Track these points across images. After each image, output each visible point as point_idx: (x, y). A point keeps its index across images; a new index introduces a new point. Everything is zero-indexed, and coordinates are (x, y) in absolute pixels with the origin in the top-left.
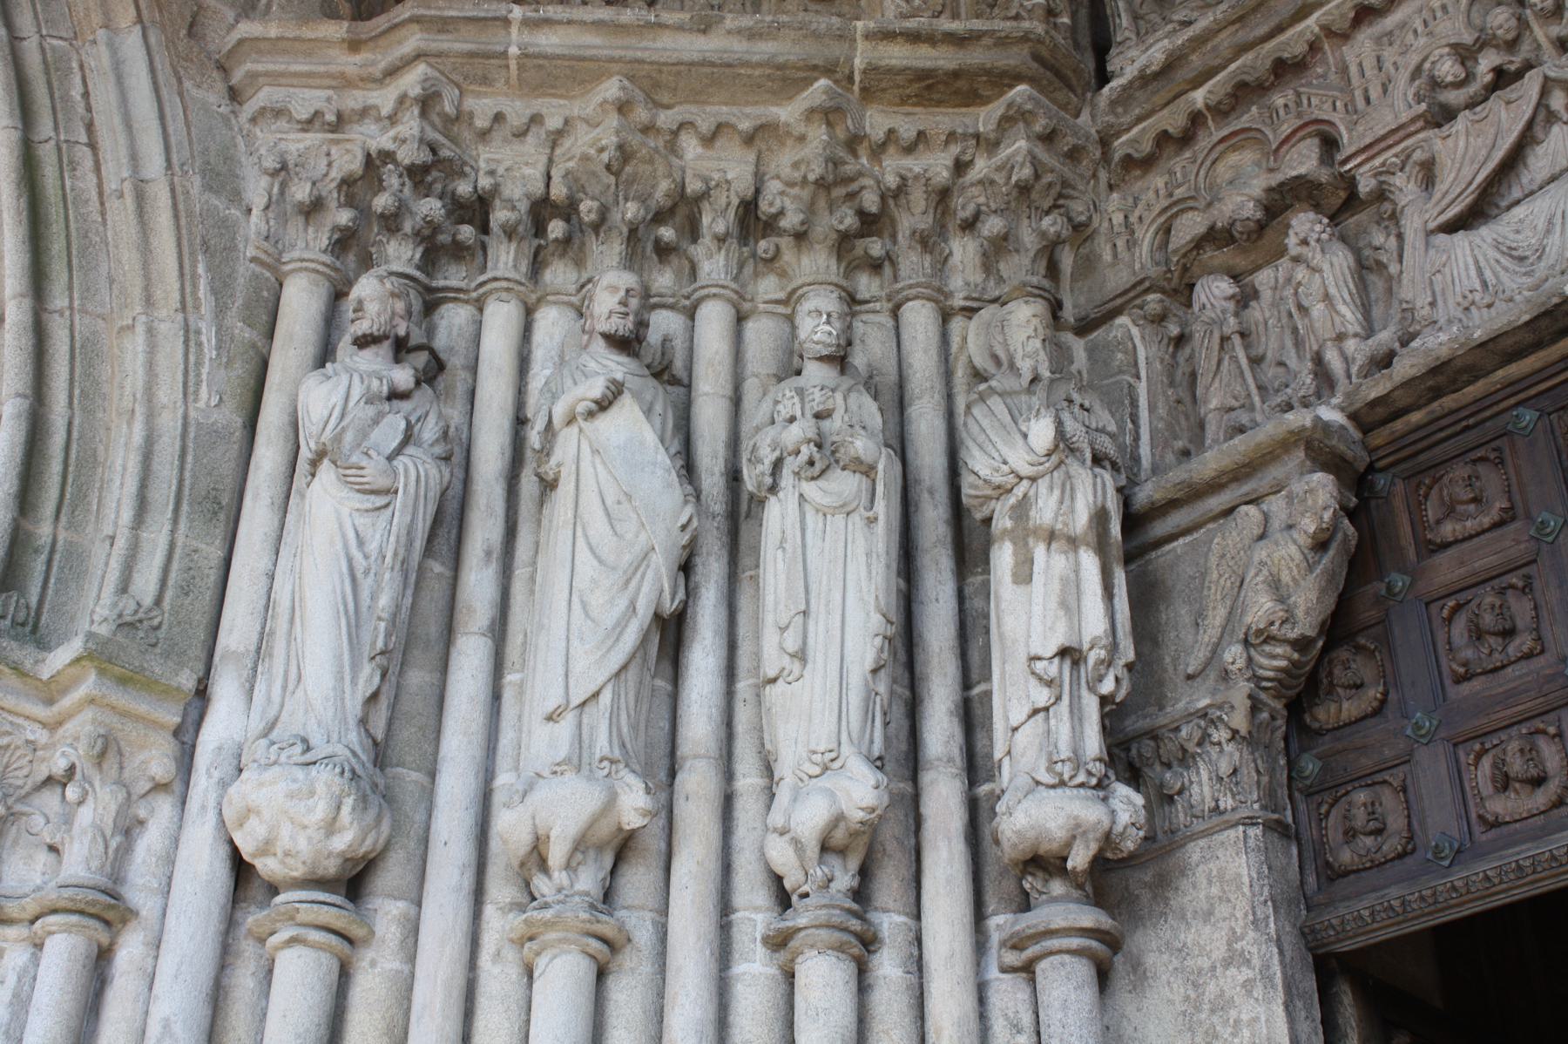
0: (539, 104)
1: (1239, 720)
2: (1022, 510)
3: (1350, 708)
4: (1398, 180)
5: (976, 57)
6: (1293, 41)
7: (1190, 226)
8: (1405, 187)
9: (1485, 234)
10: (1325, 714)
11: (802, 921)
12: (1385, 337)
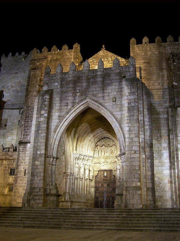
7: (96, 162)
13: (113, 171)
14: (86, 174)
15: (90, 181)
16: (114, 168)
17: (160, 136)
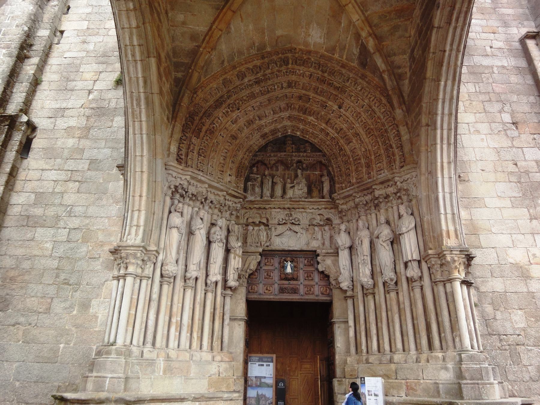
0: (198, 184)
1: (247, 277)
2: (235, 251)
5: (240, 195)
6: (267, 206)
7: (250, 220)
8: (273, 229)
10: (251, 276)
11: (210, 289)
12: (268, 244)
13: (318, 255)
15: (229, 292)
16: (323, 244)
17: (513, 123)
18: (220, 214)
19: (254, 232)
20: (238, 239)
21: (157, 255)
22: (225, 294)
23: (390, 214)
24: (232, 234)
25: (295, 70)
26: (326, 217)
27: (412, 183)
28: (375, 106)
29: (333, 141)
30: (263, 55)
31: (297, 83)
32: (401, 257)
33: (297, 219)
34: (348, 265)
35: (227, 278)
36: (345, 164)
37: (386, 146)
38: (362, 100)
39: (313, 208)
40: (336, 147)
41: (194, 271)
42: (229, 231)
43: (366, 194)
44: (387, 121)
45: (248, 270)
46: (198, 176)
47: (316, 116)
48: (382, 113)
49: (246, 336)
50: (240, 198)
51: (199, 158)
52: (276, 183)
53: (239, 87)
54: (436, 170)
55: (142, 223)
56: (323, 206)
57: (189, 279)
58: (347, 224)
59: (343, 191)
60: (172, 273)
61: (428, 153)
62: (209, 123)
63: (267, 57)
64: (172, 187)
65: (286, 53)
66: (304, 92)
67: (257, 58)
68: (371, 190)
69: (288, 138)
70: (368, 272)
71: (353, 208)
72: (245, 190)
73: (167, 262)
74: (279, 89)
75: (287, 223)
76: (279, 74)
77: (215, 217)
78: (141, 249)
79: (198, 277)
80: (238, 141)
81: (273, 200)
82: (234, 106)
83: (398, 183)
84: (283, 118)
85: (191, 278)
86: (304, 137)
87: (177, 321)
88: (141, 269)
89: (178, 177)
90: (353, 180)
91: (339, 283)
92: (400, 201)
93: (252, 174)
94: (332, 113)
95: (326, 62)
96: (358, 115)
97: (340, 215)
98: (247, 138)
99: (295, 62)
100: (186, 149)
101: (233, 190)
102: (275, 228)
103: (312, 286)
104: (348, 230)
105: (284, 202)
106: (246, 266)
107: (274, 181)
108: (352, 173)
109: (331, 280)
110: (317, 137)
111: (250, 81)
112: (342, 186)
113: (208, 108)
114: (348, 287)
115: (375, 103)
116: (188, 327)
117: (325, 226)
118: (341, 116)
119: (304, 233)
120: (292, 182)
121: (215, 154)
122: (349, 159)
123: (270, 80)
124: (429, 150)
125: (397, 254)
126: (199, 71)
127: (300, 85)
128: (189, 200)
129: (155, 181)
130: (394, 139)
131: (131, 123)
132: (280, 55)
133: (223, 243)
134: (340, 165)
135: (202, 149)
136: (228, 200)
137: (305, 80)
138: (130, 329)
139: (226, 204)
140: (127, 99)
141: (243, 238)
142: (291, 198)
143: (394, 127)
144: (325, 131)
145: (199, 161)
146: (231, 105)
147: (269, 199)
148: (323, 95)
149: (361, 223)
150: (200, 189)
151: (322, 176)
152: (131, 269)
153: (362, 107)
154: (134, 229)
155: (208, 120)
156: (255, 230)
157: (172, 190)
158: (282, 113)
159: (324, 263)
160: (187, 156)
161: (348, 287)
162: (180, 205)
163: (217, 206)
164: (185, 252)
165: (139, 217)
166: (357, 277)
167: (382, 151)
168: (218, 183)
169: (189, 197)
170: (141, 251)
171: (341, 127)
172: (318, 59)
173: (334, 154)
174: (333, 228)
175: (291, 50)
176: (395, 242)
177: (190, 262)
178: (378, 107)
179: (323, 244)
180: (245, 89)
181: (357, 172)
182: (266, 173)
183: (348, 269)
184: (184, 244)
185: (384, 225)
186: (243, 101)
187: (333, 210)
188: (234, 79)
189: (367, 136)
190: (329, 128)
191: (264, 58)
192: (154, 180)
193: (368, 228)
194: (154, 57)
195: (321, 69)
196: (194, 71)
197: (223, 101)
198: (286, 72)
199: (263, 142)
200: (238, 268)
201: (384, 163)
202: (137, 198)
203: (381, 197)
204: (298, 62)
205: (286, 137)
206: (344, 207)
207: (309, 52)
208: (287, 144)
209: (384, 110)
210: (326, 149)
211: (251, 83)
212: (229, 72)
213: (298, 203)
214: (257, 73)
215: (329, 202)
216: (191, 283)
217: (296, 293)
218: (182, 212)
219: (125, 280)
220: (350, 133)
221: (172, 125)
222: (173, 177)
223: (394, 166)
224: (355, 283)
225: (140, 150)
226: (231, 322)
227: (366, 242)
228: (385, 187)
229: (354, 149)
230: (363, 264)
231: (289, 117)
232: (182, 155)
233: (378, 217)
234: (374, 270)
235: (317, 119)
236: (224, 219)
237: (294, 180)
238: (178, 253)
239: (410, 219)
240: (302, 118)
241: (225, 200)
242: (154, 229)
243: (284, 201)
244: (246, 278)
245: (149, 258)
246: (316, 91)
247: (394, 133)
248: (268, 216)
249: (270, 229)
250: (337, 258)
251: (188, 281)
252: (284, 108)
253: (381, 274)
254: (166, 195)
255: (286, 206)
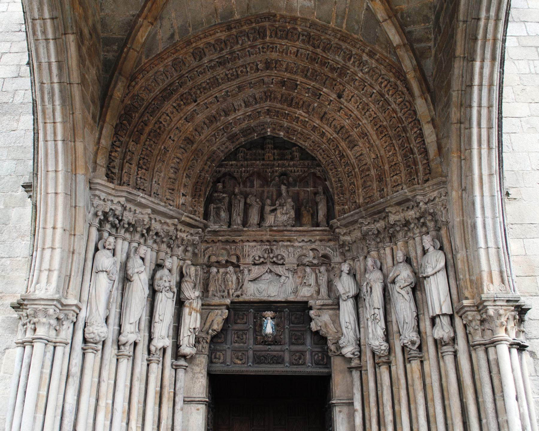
0: (136, 208)
1: (208, 341)
2: (191, 303)
3: (219, 341)
4: (246, 269)
7: (213, 259)
8: (246, 272)
9: (256, 286)
10: (215, 340)
12: (239, 293)
13: (311, 308)
14: (157, 318)
15: (182, 362)
16: (318, 292)
18: (169, 250)
19: (220, 276)
20: (195, 287)
21: (78, 311)
22: (176, 366)
23: (412, 249)
24: (187, 279)
25: (275, 45)
26: (322, 252)
27: (440, 204)
28: (388, 95)
29: (331, 144)
30: (229, 26)
31: (279, 63)
32: (426, 310)
33: (280, 257)
34: (352, 322)
35: (180, 343)
36: (348, 177)
37: (404, 151)
38: (371, 86)
39: (303, 241)
40: (335, 152)
41: (132, 333)
42: (182, 275)
43: (378, 219)
44: (406, 115)
45: (210, 331)
46: (136, 197)
47: (306, 109)
48: (399, 105)
49: (208, 425)
50: (198, 227)
51: (139, 172)
52: (250, 205)
53: (196, 69)
54: (472, 185)
55: (56, 265)
56: (318, 237)
57: (124, 345)
58: (351, 263)
59: (346, 215)
60: (100, 336)
61: (461, 162)
62: (153, 122)
63: (235, 28)
64: (100, 213)
65: (262, 22)
66: (288, 75)
67: (221, 29)
68: (384, 215)
69: (268, 141)
70: (380, 332)
71: (360, 239)
72: (206, 216)
73: (92, 320)
74: (253, 71)
75: (266, 263)
76: (252, 50)
77: (162, 255)
78: (55, 303)
79: (137, 341)
80: (195, 146)
81: (245, 229)
82: (190, 97)
83: (421, 204)
84: (259, 113)
85: (127, 342)
86: (290, 138)
87: (107, 404)
88: (55, 331)
89: (108, 200)
90: (359, 200)
91: (339, 348)
92: (424, 229)
93: (216, 192)
94: (329, 104)
95: (318, 33)
96: (365, 108)
97: (341, 250)
98: (208, 141)
99: (275, 33)
100: (120, 159)
101: (188, 217)
102: (249, 271)
103: (302, 353)
104: (352, 271)
105: (262, 233)
106: (208, 324)
107: (248, 201)
108: (358, 190)
109: (330, 344)
110: (309, 138)
111: (211, 61)
112: (343, 209)
113: (152, 101)
114: (353, 354)
115: (389, 90)
116: (123, 413)
117: (321, 265)
118: (341, 108)
119: (290, 276)
120: (273, 204)
121: (162, 165)
122: (354, 169)
123: (239, 59)
124: (463, 157)
125: (421, 306)
126: (138, 50)
127: (283, 65)
128: (125, 232)
129: (75, 207)
130: (415, 141)
131: (41, 125)
132: (254, 25)
133: (174, 293)
134: (341, 179)
135: (144, 158)
136: (181, 231)
137: (290, 59)
138: (40, 416)
139: (178, 237)
140: (35, 92)
141: (204, 285)
142: (272, 226)
143: (415, 124)
144: (320, 130)
145: (139, 176)
146: (185, 96)
147: (241, 227)
148: (316, 79)
149: (370, 262)
150: (140, 216)
151: (315, 194)
152: (41, 332)
153: (371, 96)
154: (45, 274)
155: (152, 118)
156: (221, 273)
157: (99, 217)
158: (258, 105)
159: (319, 318)
160: (122, 170)
161: (353, 354)
162: (111, 239)
163: (165, 240)
164: (118, 306)
165: (52, 257)
166: (365, 339)
167: (400, 158)
168: (165, 207)
169: (124, 227)
170: (55, 305)
171: (342, 125)
172: (307, 29)
173: (332, 162)
174: (333, 268)
175: (268, 18)
176: (418, 288)
177: (125, 320)
178: (392, 95)
179: (318, 292)
180: (204, 72)
181: (365, 188)
182: (237, 190)
183: (353, 327)
184: (116, 294)
185: (402, 264)
186: (202, 90)
187: (331, 244)
188: (189, 59)
189: (378, 136)
190: (325, 126)
191: (231, 28)
192: (74, 205)
193: (381, 269)
194: (73, 33)
195: (311, 43)
196: (131, 50)
197: (174, 90)
198: (263, 48)
199: (232, 147)
200: (194, 329)
201: (403, 175)
202: (49, 231)
203: (398, 223)
204: (279, 34)
205: (264, 138)
206: (348, 238)
207: (294, 19)
208: (266, 148)
209: (401, 99)
210: (321, 155)
211: (213, 65)
212: (182, 49)
213: (281, 234)
214: (222, 50)
215: (325, 231)
216: (127, 350)
217: (280, 363)
218: (114, 250)
219: (33, 346)
220: (354, 133)
221: (100, 125)
222: (100, 199)
223: (416, 180)
224: (362, 347)
225: (54, 163)
226: (186, 406)
227: (378, 289)
228: (403, 210)
229: (361, 155)
230: (373, 320)
231: (268, 110)
232: (114, 167)
233: (394, 254)
234: (390, 328)
235: (307, 112)
236: (175, 258)
237: (276, 201)
238: (108, 308)
239: (438, 256)
240: (287, 112)
241: (177, 230)
242: (73, 274)
243: (262, 231)
244: (207, 342)
245: (66, 315)
246: (306, 75)
247: (415, 132)
248: (238, 252)
249: (242, 272)
250: (338, 311)
251: (122, 347)
252: (261, 98)
253: (399, 334)
254: (90, 225)
255: (265, 238)
